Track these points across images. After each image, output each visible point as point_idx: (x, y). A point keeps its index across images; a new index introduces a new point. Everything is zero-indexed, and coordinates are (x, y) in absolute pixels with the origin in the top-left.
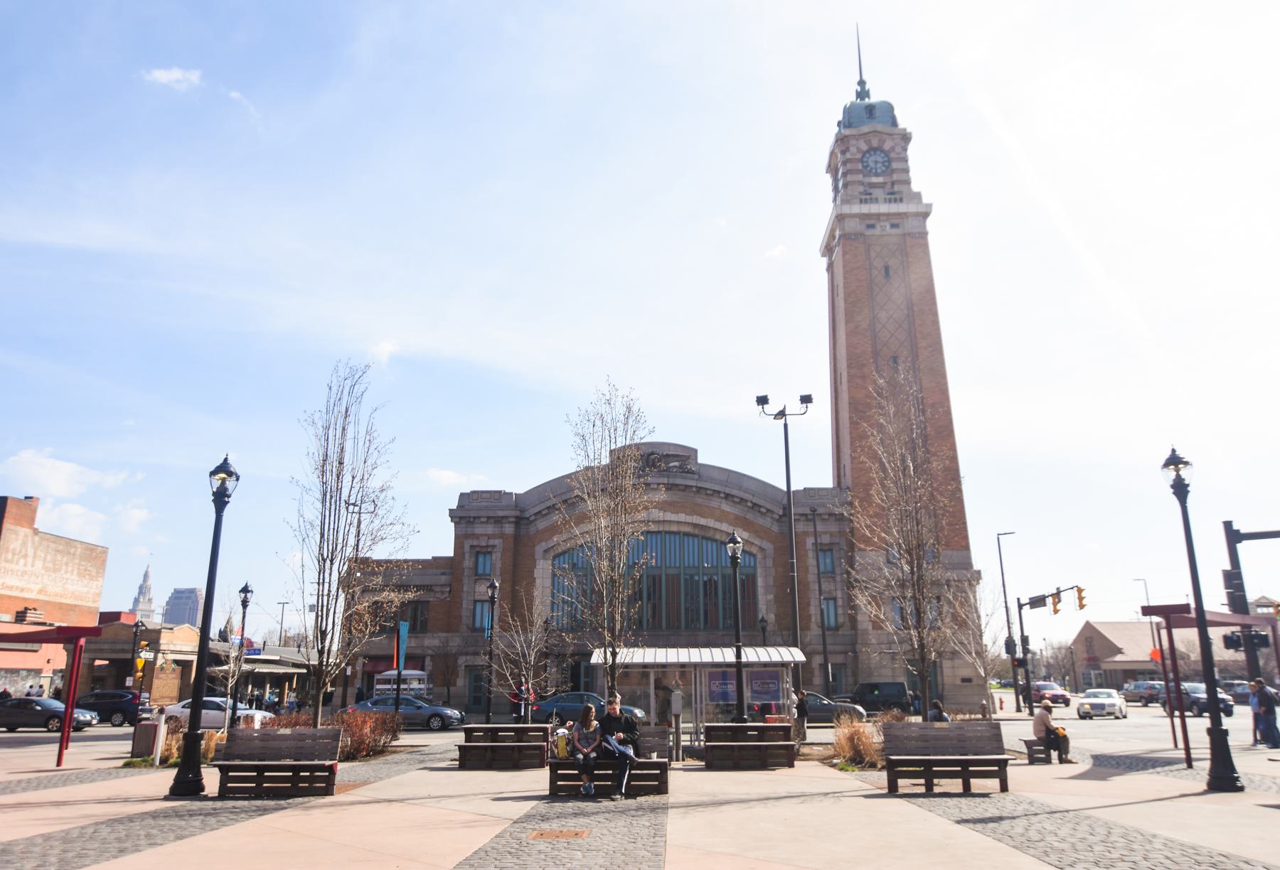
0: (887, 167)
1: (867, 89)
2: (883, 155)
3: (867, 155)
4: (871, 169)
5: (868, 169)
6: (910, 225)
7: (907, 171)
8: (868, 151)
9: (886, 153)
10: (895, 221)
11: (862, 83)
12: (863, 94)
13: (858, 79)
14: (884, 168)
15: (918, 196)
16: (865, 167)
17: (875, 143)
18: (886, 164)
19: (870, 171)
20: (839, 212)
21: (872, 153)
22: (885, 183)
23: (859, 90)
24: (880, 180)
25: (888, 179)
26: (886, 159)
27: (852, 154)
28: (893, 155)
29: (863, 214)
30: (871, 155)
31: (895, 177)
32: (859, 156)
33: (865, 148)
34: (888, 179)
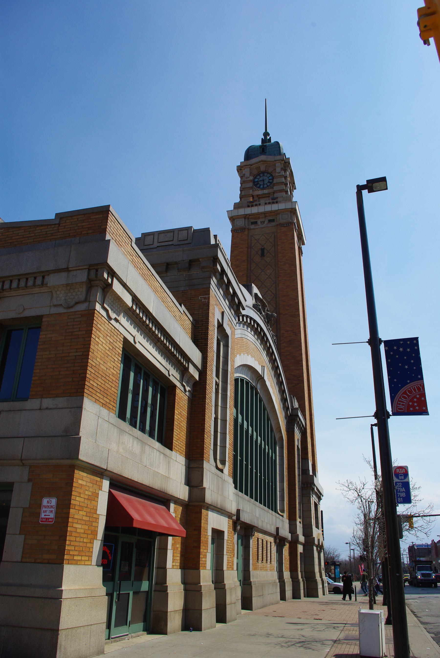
0: (271, 183)
1: (268, 138)
2: (269, 175)
3: (258, 177)
4: (260, 185)
5: (258, 186)
10: (271, 218)
11: (266, 134)
14: (268, 184)
20: (230, 216)
23: (264, 139)
24: (266, 191)
25: (271, 191)
26: (271, 178)
28: (273, 175)
30: (260, 177)
32: (251, 178)
34: (271, 191)
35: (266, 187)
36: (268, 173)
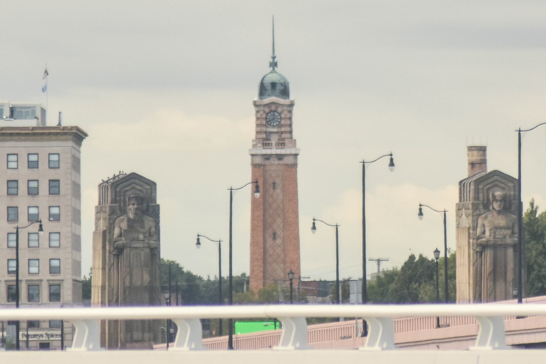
2: (277, 115)
5: (270, 123)
6: (289, 160)
7: (290, 125)
8: (270, 112)
11: (274, 58)
12: (274, 65)
13: (271, 54)
14: (277, 123)
15: (294, 142)
16: (267, 122)
17: (273, 108)
18: (279, 120)
19: (270, 124)
24: (275, 130)
26: (279, 117)
28: (283, 116)
31: (283, 129)
33: (267, 110)
35: (275, 126)
36: (277, 112)
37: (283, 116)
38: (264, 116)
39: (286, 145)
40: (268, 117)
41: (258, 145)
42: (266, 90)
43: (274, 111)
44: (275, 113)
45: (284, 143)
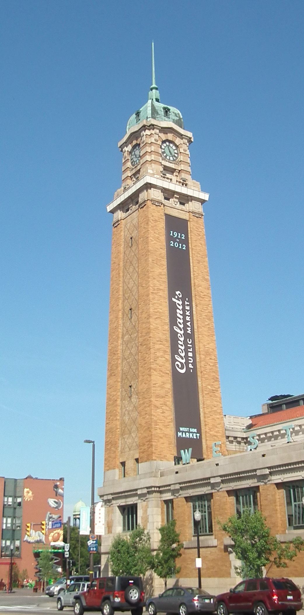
2: (174, 148)
4: (167, 155)
5: (165, 155)
9: (177, 146)
17: (170, 136)
18: (176, 155)
19: (166, 157)
21: (167, 143)
22: (175, 170)
26: (176, 151)
27: (155, 140)
29: (164, 188)
31: (182, 167)
37: (182, 150)
38: (160, 143)
39: (189, 186)
40: (163, 147)
41: (155, 176)
42: (158, 114)
43: (170, 142)
44: (171, 145)
45: (186, 185)
